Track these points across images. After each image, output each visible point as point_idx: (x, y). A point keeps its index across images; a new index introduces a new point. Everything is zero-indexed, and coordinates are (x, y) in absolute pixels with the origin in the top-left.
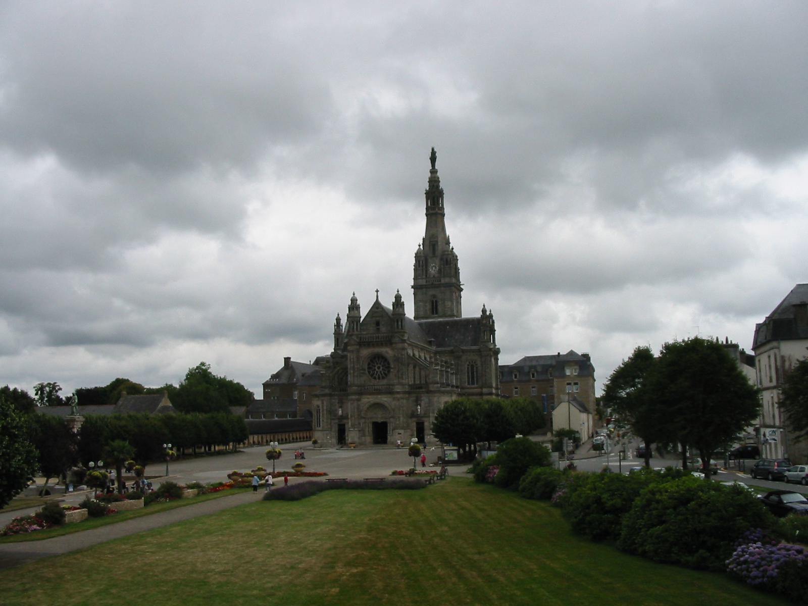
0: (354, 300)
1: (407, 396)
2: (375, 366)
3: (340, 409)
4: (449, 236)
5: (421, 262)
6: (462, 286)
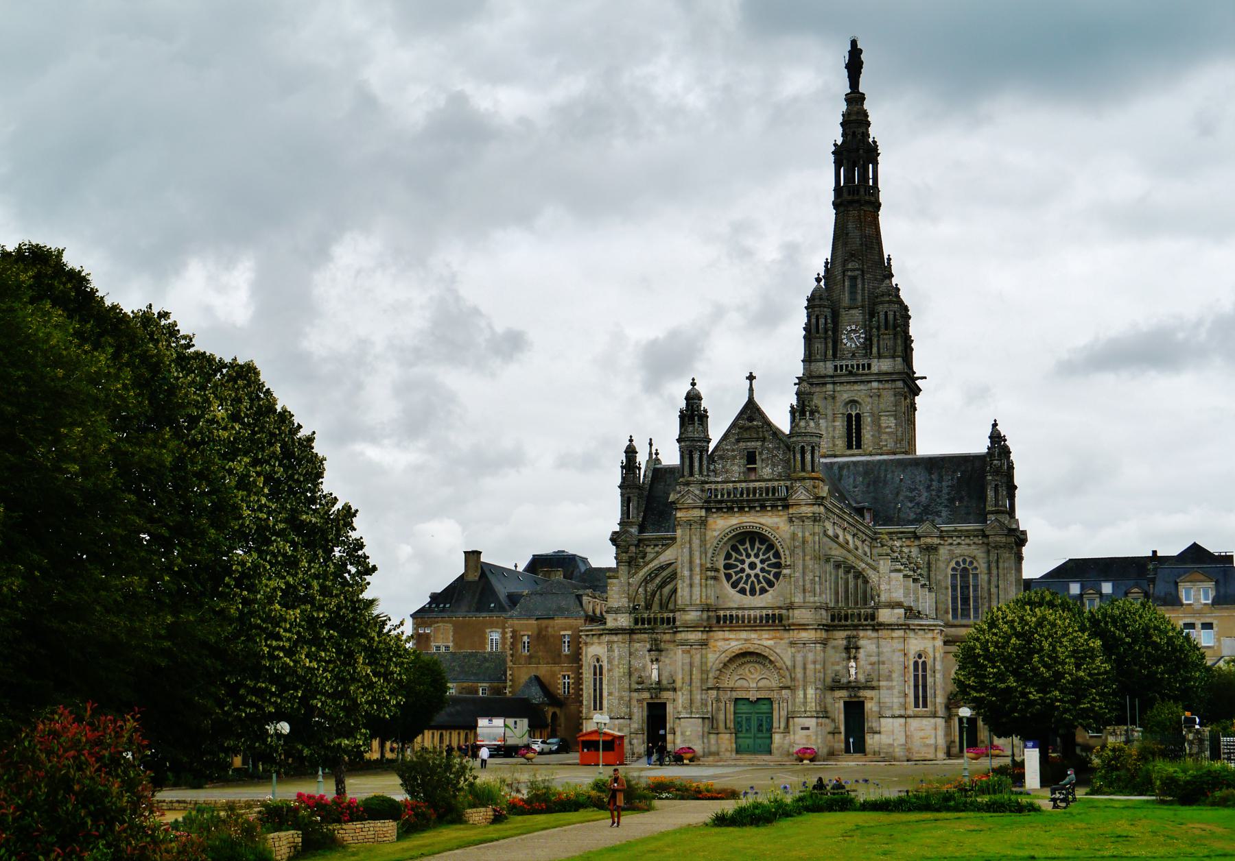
0: (693, 398)
1: (824, 635)
2: (743, 562)
3: (655, 666)
4: (889, 259)
5: (822, 321)
6: (918, 382)
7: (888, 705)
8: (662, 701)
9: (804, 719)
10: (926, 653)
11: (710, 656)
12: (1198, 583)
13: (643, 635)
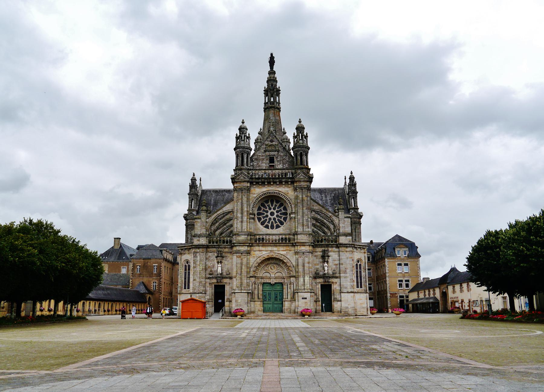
2: (267, 212)
3: (220, 265)
4: (284, 129)
7: (345, 286)
8: (223, 284)
9: (304, 293)
10: (361, 260)
11: (251, 259)
12: (402, 249)
13: (213, 249)
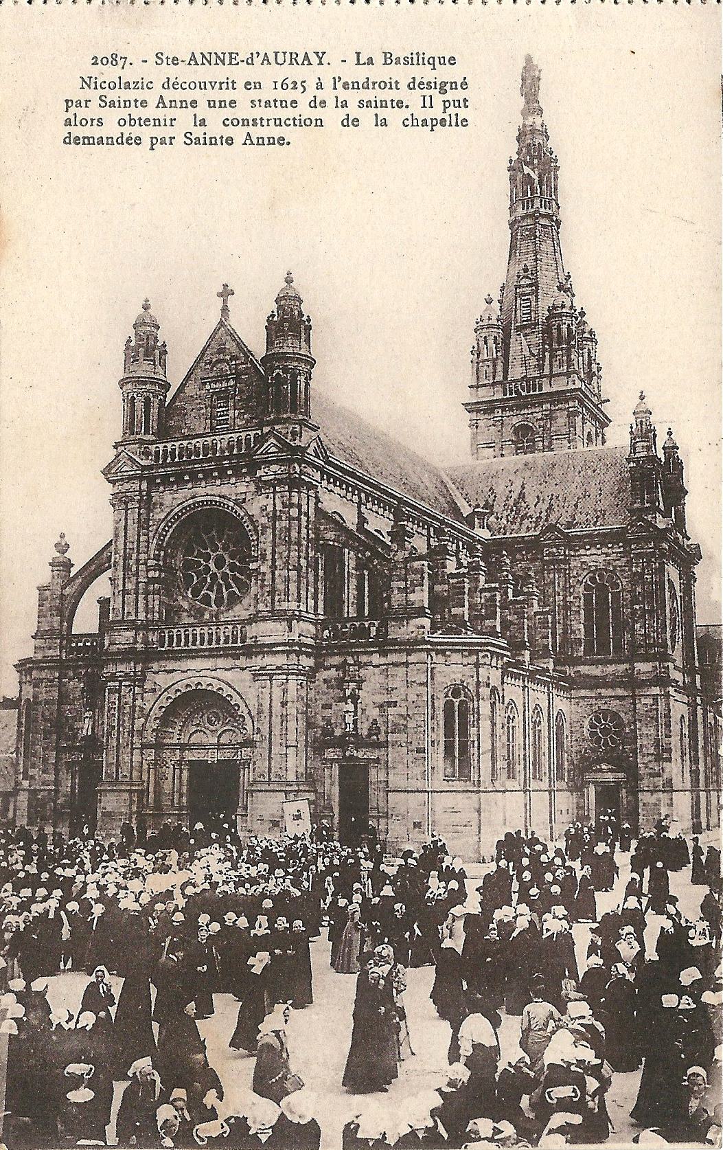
1: (307, 662)
